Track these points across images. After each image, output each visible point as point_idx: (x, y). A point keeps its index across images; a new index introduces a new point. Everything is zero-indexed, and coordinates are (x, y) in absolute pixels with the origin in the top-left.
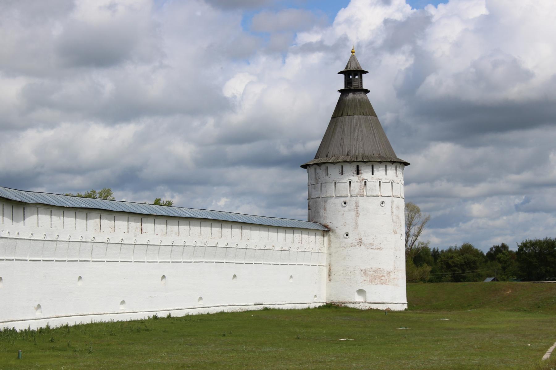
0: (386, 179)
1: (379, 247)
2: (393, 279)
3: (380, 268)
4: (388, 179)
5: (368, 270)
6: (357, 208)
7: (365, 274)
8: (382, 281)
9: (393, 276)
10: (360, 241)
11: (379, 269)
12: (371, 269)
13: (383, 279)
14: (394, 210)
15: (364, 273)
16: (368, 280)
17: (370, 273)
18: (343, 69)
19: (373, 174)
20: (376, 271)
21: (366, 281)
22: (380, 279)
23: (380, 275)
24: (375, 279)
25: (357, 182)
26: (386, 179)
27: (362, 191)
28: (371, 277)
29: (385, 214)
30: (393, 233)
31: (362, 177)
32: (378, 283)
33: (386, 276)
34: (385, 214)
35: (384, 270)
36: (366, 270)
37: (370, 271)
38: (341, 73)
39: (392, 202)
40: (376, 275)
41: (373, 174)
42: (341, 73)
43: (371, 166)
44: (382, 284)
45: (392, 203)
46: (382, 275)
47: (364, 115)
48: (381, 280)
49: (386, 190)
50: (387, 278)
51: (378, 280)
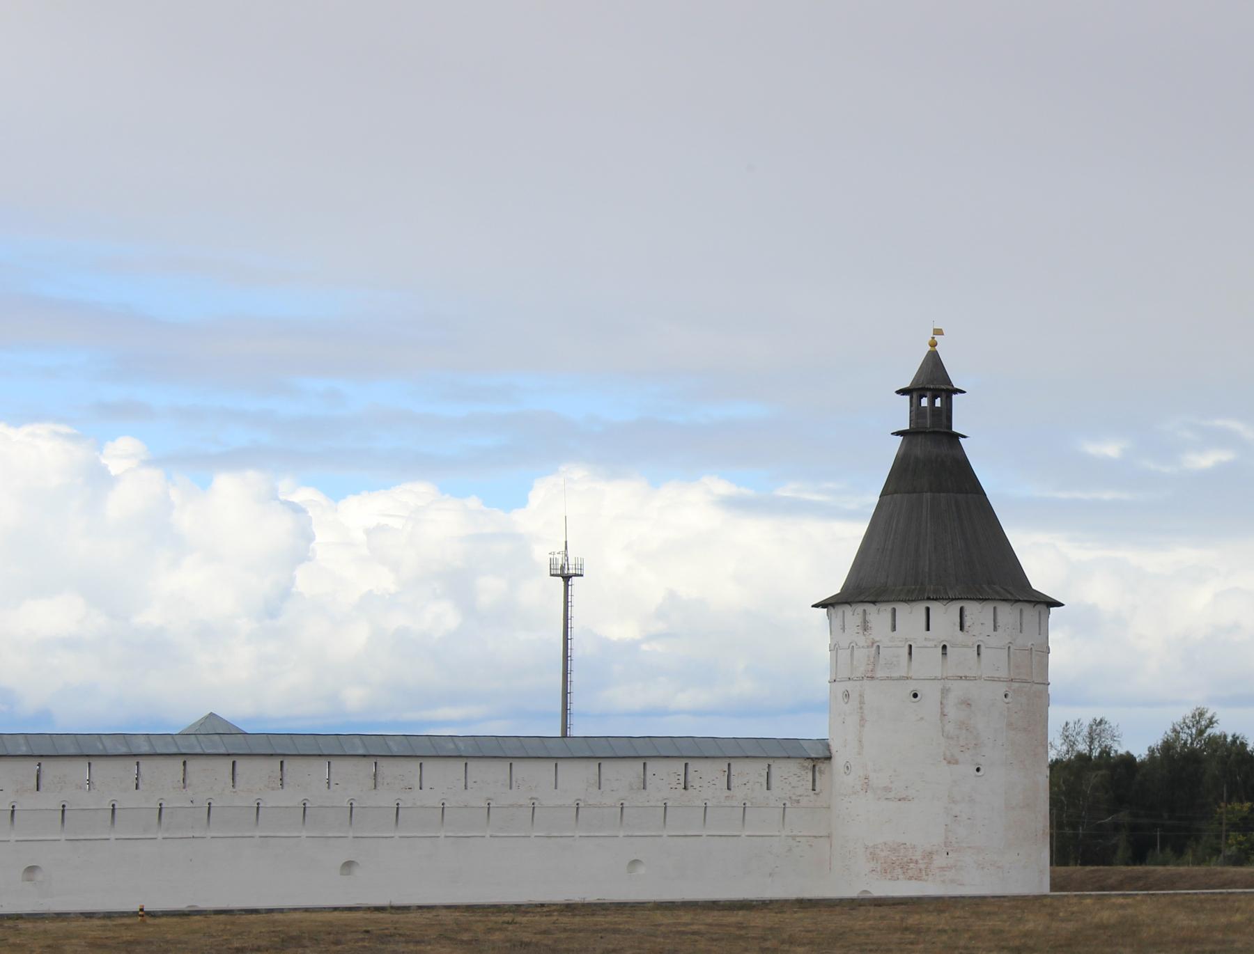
0: (926, 639)
1: (904, 796)
2: (942, 869)
3: (905, 844)
4: (933, 640)
5: (880, 846)
6: (861, 708)
7: (873, 857)
8: (910, 873)
9: (939, 861)
10: (866, 781)
11: (902, 847)
12: (885, 844)
13: (912, 868)
14: (952, 712)
15: (871, 853)
16: (879, 869)
17: (883, 854)
18: (907, 384)
19: (894, 628)
20: (895, 849)
21: (874, 873)
22: (904, 867)
23: (905, 859)
24: (894, 869)
25: (863, 647)
26: (926, 639)
27: (870, 667)
28: (885, 863)
29: (922, 719)
30: (945, 762)
31: (871, 636)
32: (900, 877)
33: (920, 862)
34: (922, 719)
35: (914, 847)
36: (875, 847)
37: (882, 850)
38: (902, 392)
39: (945, 692)
40: (894, 859)
41: (894, 628)
42: (902, 392)
43: (842, 611)
44: (910, 878)
45: (942, 693)
46: (911, 859)
47: (914, 492)
48: (907, 869)
49: (928, 662)
50: (923, 866)
51: (900, 870)
